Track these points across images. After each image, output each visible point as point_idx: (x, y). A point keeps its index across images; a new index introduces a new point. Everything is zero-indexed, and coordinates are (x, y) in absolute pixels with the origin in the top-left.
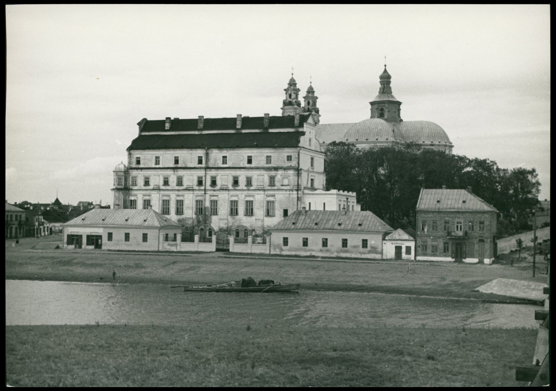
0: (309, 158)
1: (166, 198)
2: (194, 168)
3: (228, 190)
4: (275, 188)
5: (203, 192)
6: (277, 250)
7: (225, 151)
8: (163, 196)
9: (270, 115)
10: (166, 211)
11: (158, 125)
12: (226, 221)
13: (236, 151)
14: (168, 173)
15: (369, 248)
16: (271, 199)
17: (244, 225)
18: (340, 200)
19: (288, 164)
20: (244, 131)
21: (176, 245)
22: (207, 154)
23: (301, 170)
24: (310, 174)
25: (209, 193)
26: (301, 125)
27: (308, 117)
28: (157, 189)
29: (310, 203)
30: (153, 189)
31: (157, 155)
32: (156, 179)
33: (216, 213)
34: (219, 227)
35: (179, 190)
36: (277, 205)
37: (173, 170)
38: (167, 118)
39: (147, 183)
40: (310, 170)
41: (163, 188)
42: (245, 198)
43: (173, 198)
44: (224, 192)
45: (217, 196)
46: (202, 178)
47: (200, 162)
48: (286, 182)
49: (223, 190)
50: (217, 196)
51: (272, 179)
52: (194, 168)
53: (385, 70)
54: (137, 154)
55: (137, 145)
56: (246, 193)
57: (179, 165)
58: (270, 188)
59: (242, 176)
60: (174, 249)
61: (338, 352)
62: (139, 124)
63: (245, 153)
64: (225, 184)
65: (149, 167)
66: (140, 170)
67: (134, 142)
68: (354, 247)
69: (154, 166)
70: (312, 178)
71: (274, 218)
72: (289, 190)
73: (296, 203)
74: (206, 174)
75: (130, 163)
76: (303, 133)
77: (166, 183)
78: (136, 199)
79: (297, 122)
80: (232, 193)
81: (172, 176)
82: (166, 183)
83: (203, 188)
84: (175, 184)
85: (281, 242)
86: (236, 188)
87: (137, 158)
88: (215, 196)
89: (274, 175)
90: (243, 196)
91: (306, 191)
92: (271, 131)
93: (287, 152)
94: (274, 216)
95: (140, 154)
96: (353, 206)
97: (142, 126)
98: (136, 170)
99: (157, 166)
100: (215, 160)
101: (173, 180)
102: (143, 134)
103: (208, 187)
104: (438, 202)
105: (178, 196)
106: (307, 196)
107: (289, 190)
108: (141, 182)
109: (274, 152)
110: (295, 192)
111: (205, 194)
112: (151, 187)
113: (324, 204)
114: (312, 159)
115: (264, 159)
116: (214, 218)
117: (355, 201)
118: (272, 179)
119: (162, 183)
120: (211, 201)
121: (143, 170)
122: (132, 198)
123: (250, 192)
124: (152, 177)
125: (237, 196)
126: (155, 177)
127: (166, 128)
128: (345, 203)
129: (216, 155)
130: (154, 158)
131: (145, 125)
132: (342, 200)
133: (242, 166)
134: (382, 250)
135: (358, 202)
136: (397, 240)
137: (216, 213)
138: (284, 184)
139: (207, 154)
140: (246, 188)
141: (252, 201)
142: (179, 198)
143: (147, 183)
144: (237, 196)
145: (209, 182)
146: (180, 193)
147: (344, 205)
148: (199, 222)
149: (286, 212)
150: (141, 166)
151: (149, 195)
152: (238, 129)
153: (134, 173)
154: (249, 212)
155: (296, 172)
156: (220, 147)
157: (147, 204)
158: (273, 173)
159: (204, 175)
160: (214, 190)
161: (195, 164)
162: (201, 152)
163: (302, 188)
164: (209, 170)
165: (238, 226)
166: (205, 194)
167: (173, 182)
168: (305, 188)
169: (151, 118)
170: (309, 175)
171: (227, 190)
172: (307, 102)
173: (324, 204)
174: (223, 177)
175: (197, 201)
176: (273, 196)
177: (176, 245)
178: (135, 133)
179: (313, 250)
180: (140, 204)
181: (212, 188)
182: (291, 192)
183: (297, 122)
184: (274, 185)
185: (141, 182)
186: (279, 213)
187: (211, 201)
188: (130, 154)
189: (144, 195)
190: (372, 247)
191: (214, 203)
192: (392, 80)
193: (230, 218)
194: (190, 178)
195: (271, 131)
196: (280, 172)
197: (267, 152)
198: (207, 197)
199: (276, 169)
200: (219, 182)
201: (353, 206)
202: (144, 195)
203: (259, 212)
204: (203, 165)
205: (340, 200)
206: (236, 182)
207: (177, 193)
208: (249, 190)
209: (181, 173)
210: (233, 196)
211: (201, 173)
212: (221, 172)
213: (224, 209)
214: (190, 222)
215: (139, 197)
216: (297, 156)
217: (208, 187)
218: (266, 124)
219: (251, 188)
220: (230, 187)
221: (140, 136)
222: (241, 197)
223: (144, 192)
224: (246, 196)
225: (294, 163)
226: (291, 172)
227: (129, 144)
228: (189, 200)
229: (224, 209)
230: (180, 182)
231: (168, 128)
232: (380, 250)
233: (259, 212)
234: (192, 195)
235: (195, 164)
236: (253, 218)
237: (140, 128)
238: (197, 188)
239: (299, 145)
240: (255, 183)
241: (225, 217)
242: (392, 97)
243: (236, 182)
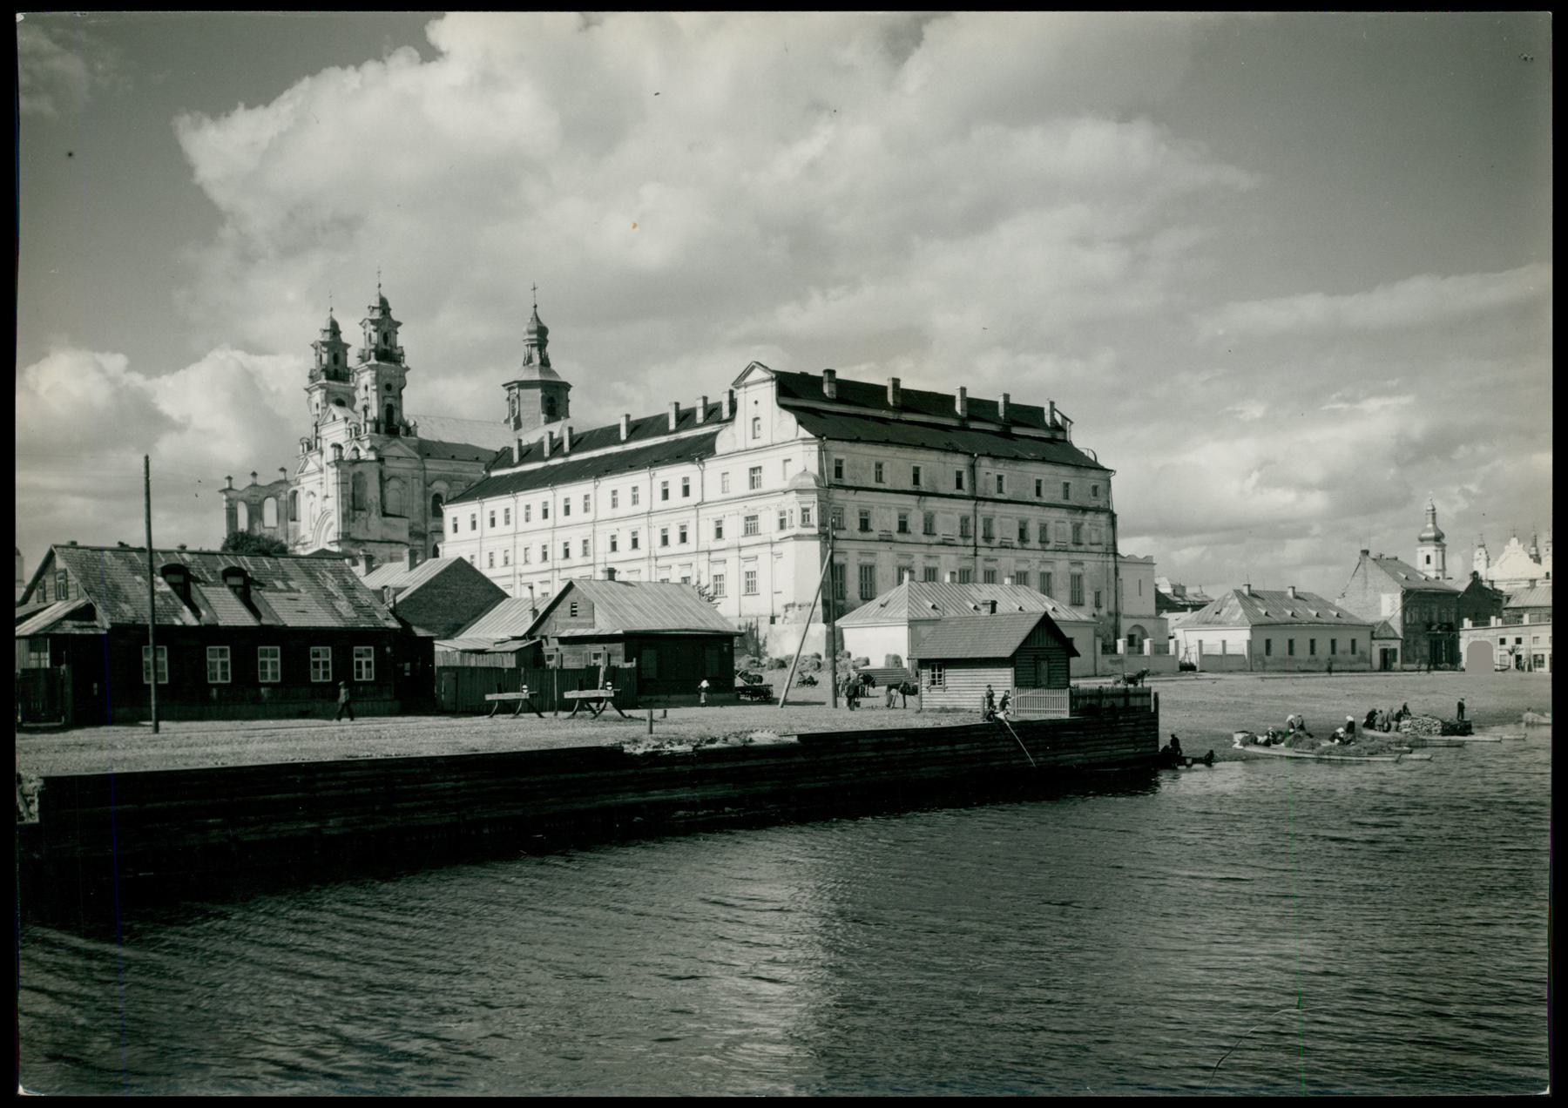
2: (952, 496)
4: (1082, 548)
5: (970, 551)
6: (1259, 663)
7: (1001, 465)
13: (1018, 468)
14: (907, 502)
15: (1358, 654)
16: (1077, 570)
19: (1094, 503)
20: (974, 425)
22: (972, 467)
25: (981, 552)
28: (886, 539)
31: (880, 460)
32: (885, 514)
35: (930, 545)
36: (1086, 582)
37: (918, 497)
39: (865, 526)
41: (897, 537)
42: (1039, 567)
45: (996, 560)
47: (959, 485)
48: (1095, 539)
49: (1006, 547)
50: (996, 560)
51: (1077, 528)
52: (952, 496)
53: (536, 314)
56: (1040, 555)
57: (924, 485)
58: (1074, 548)
59: (1034, 516)
65: (864, 486)
66: (853, 492)
68: (1344, 652)
69: (873, 484)
71: (1083, 609)
73: (1113, 580)
74: (975, 511)
77: (903, 527)
78: (843, 561)
80: (1021, 554)
81: (915, 510)
82: (903, 527)
83: (970, 542)
84: (921, 530)
86: (1025, 545)
87: (836, 460)
88: (992, 560)
89: (1079, 521)
90: (1036, 562)
94: (1082, 605)
95: (843, 452)
98: (844, 491)
99: (881, 486)
100: (986, 484)
103: (981, 542)
105: (929, 557)
108: (853, 523)
109: (1075, 477)
110: (1111, 558)
111: (976, 555)
112: (874, 535)
115: (1060, 487)
118: (1077, 528)
119: (895, 527)
121: (859, 492)
123: (1049, 555)
124: (875, 511)
126: (883, 510)
130: (873, 466)
134: (1371, 656)
136: (1382, 639)
139: (972, 467)
140: (1038, 546)
143: (865, 526)
145: (980, 533)
146: (935, 550)
149: (1098, 594)
150: (848, 481)
151: (872, 554)
153: (839, 496)
155: (1110, 520)
158: (1078, 517)
159: (972, 512)
161: (950, 488)
162: (960, 462)
164: (982, 503)
166: (976, 555)
167: (917, 525)
172: (332, 354)
174: (1003, 520)
176: (1080, 563)
179: (1300, 661)
181: (986, 544)
182: (1104, 559)
184: (1079, 544)
186: (1089, 598)
190: (1362, 652)
192: (548, 337)
196: (1089, 517)
199: (1085, 510)
200: (997, 531)
202: (861, 553)
204: (966, 491)
206: (1023, 535)
207: (924, 549)
209: (932, 504)
211: (966, 507)
216: (1106, 487)
217: (981, 542)
219: (1049, 547)
220: (1016, 544)
223: (862, 546)
225: (1101, 503)
226: (1103, 518)
230: (929, 530)
231: (835, 396)
232: (1368, 657)
234: (953, 558)
235: (950, 488)
240: (1051, 535)
242: (553, 373)
243: (1023, 535)
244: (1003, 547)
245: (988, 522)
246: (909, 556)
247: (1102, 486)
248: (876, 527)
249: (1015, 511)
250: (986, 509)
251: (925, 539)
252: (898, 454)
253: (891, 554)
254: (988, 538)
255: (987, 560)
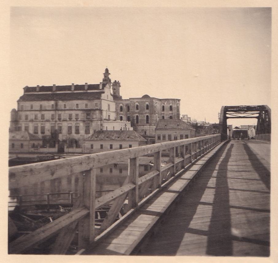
0: (107, 105)
1: (36, 125)
3: (67, 121)
8: (35, 124)
9: (88, 84)
10: (36, 132)
11: (34, 89)
12: (65, 137)
17: (75, 138)
18: (122, 125)
21: (38, 149)
23: (102, 110)
24: (108, 112)
26: (103, 89)
27: (106, 84)
28: (32, 121)
29: (107, 127)
30: (30, 121)
32: (31, 115)
33: (61, 133)
34: (63, 140)
35: (42, 121)
38: (37, 86)
40: (108, 110)
43: (40, 125)
44: (65, 122)
45: (61, 124)
46: (54, 115)
54: (22, 103)
55: (23, 99)
56: (75, 122)
59: (74, 113)
60: (36, 151)
61: (63, 220)
62: (24, 89)
63: (75, 102)
64: (65, 118)
67: (21, 98)
70: (109, 114)
72: (97, 120)
75: (18, 108)
76: (104, 93)
79: (101, 87)
83: (54, 120)
84: (40, 119)
85: (90, 147)
88: (60, 124)
90: (74, 124)
91: (105, 121)
92: (89, 91)
93: (96, 101)
96: (129, 128)
97: (25, 90)
101: (39, 116)
102: (26, 93)
104: (166, 125)
105: (42, 124)
106: (105, 123)
107: (97, 120)
108: (23, 118)
112: (29, 120)
113: (114, 127)
114: (109, 105)
115: (84, 105)
116: (60, 135)
117: (130, 126)
120: (59, 126)
122: (19, 126)
125: (71, 124)
127: (37, 91)
128: (125, 127)
129: (61, 103)
131: (27, 89)
132: (123, 125)
133: (73, 109)
135: (131, 126)
137: (61, 133)
138: (94, 117)
141: (79, 126)
142: (42, 125)
144: (71, 124)
145: (57, 118)
147: (124, 128)
148: (52, 137)
152: (72, 91)
153: (20, 113)
154: (77, 132)
156: (63, 100)
157: (27, 129)
160: (60, 121)
162: (52, 102)
163: (103, 120)
165: (72, 139)
166: (56, 123)
168: (105, 119)
169: (30, 86)
170: (107, 113)
171: (66, 121)
173: (114, 127)
175: (51, 127)
177: (38, 149)
178: (22, 93)
180: (23, 129)
182: (98, 122)
183: (101, 87)
185: (23, 118)
187: (59, 126)
188: (18, 104)
189: (25, 124)
191: (60, 128)
193: (68, 136)
194: (48, 115)
195: (89, 91)
197: (85, 102)
198: (57, 125)
200: (62, 118)
201: (129, 128)
202: (25, 124)
203: (82, 132)
205: (122, 125)
208: (77, 121)
209: (43, 113)
210: (69, 124)
211: (53, 112)
212: (63, 112)
213: (65, 131)
214: (48, 137)
215: (23, 125)
218: (86, 88)
220: (68, 120)
221: (24, 95)
222: (73, 124)
223: (26, 123)
224: (76, 124)
227: (18, 98)
228: (48, 126)
229: (65, 131)
233: (82, 132)
236: (79, 135)
237: (24, 90)
238: (51, 120)
239: (101, 98)
241: (66, 134)
244: (64, 121)
245: (60, 115)
246: (37, 124)
247: (99, 103)
248: (29, 118)
249: (68, 112)
250: (60, 112)
251: (42, 120)
252: (37, 102)
253: (32, 124)
254: (59, 119)
255: (58, 124)
